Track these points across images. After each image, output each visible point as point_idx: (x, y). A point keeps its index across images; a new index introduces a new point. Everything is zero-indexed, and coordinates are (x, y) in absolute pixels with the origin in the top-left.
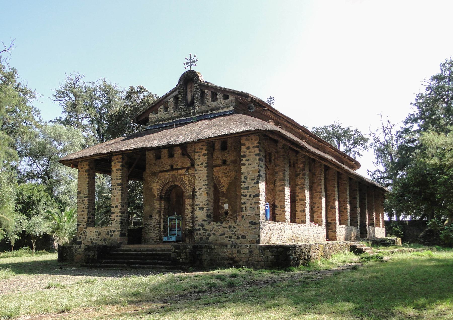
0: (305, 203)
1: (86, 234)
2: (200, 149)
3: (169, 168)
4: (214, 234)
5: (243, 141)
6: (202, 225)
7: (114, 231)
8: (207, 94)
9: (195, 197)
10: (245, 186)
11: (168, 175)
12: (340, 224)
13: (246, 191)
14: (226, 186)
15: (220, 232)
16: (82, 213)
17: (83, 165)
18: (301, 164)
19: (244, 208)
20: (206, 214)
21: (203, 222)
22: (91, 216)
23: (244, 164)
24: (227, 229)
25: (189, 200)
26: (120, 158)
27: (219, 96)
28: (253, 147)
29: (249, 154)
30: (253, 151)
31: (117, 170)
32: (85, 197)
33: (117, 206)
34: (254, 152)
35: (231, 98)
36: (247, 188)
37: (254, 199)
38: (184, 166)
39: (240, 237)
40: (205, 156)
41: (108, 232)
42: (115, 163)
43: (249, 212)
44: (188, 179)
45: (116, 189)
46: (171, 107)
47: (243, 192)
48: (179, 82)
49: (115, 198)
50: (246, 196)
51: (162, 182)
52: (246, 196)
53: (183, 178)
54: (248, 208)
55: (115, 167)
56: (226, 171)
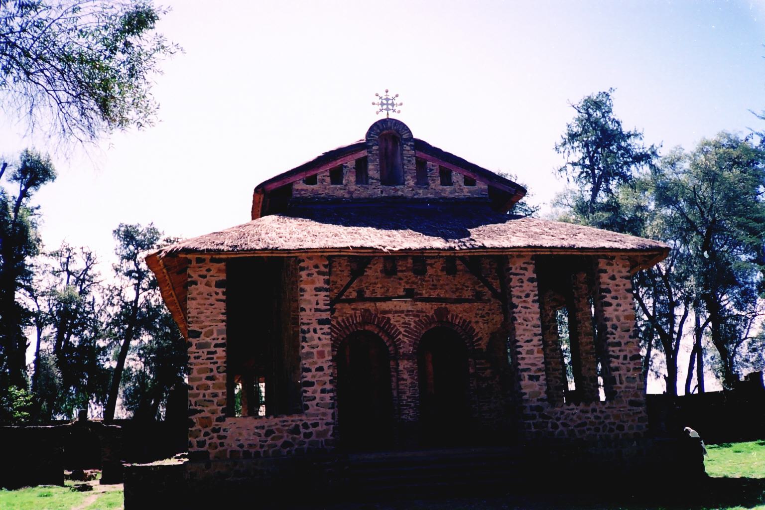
1: (222, 433)
2: (521, 269)
3: (354, 295)
4: (564, 425)
5: (602, 264)
6: (539, 409)
7: (315, 425)
8: (431, 170)
9: (520, 356)
10: (615, 341)
11: (353, 309)
13: (617, 349)
14: (486, 339)
16: (210, 383)
17: (209, 270)
19: (617, 378)
23: (610, 304)
25: (406, 362)
26: (325, 266)
27: (457, 177)
28: (622, 277)
29: (616, 288)
30: (621, 284)
32: (216, 346)
33: (320, 369)
36: (619, 344)
37: (632, 363)
38: (390, 294)
40: (532, 282)
41: (297, 426)
42: (309, 275)
43: (625, 384)
44: (402, 321)
45: (315, 331)
46: (350, 178)
47: (613, 351)
48: (368, 134)
49: (315, 351)
50: (618, 357)
51: (338, 323)
52: (618, 357)
53: (389, 319)
54: (624, 379)
55: (313, 282)
56: (484, 313)
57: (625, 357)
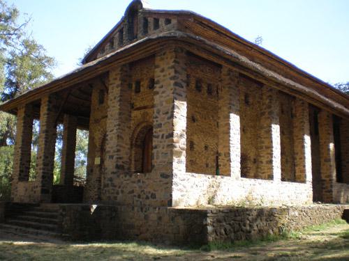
0: (272, 151)
6: (111, 180)
7: (37, 187)
12: (192, 167)
15: (129, 189)
18: (266, 99)
20: (115, 164)
21: (112, 176)
22: (24, 169)
24: (135, 185)
27: (162, 22)
28: (169, 68)
31: (44, 115)
34: (169, 74)
35: (174, 21)
39: (150, 195)
43: (161, 159)
57: (162, 137)
